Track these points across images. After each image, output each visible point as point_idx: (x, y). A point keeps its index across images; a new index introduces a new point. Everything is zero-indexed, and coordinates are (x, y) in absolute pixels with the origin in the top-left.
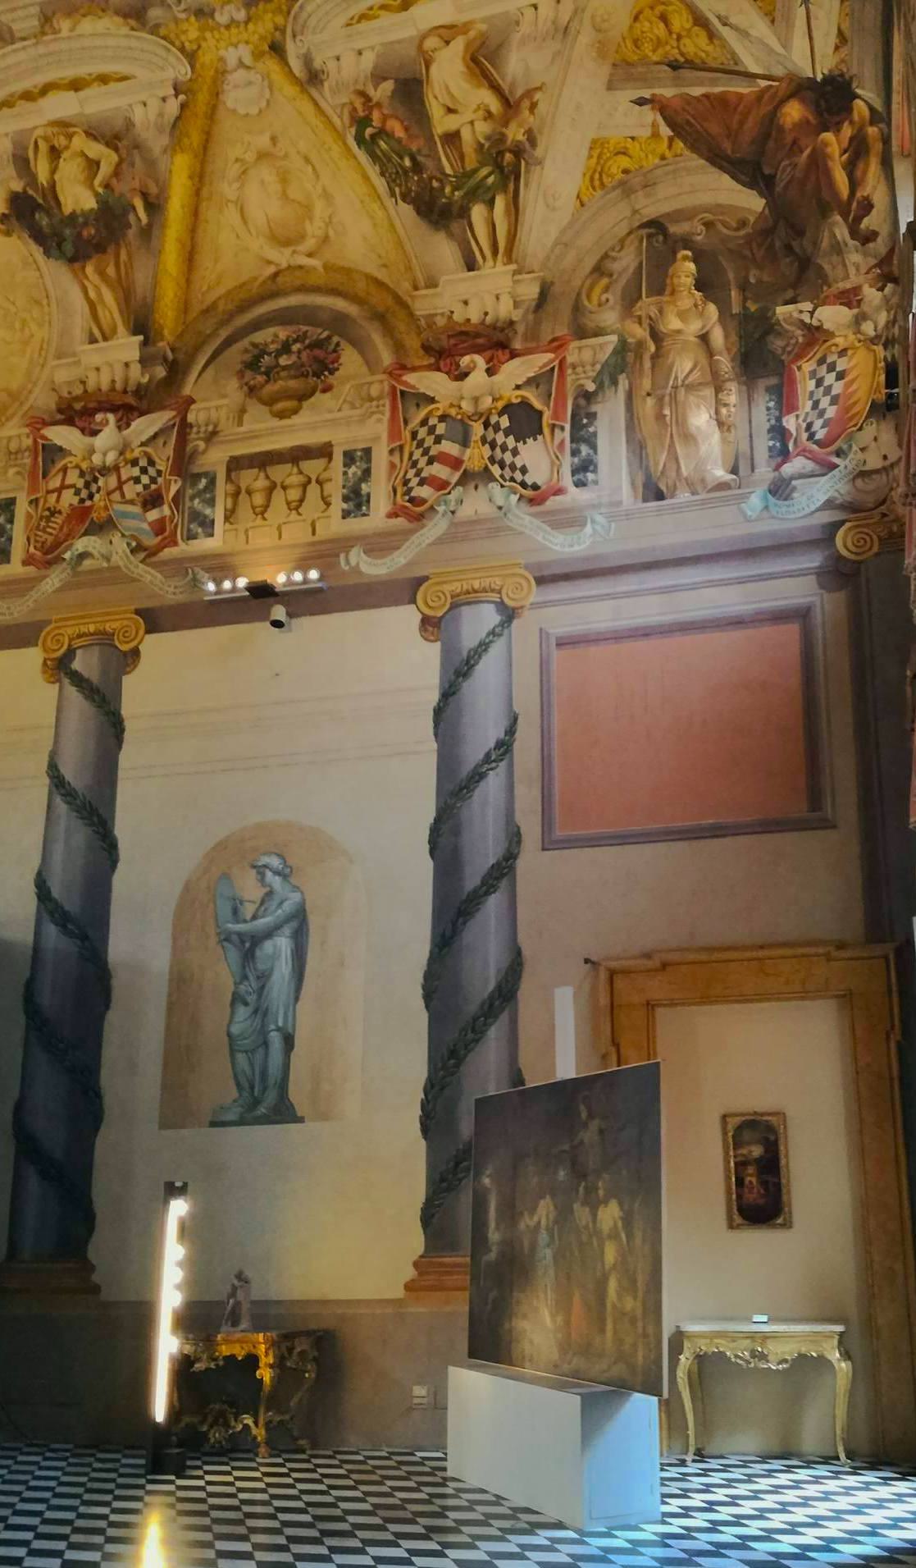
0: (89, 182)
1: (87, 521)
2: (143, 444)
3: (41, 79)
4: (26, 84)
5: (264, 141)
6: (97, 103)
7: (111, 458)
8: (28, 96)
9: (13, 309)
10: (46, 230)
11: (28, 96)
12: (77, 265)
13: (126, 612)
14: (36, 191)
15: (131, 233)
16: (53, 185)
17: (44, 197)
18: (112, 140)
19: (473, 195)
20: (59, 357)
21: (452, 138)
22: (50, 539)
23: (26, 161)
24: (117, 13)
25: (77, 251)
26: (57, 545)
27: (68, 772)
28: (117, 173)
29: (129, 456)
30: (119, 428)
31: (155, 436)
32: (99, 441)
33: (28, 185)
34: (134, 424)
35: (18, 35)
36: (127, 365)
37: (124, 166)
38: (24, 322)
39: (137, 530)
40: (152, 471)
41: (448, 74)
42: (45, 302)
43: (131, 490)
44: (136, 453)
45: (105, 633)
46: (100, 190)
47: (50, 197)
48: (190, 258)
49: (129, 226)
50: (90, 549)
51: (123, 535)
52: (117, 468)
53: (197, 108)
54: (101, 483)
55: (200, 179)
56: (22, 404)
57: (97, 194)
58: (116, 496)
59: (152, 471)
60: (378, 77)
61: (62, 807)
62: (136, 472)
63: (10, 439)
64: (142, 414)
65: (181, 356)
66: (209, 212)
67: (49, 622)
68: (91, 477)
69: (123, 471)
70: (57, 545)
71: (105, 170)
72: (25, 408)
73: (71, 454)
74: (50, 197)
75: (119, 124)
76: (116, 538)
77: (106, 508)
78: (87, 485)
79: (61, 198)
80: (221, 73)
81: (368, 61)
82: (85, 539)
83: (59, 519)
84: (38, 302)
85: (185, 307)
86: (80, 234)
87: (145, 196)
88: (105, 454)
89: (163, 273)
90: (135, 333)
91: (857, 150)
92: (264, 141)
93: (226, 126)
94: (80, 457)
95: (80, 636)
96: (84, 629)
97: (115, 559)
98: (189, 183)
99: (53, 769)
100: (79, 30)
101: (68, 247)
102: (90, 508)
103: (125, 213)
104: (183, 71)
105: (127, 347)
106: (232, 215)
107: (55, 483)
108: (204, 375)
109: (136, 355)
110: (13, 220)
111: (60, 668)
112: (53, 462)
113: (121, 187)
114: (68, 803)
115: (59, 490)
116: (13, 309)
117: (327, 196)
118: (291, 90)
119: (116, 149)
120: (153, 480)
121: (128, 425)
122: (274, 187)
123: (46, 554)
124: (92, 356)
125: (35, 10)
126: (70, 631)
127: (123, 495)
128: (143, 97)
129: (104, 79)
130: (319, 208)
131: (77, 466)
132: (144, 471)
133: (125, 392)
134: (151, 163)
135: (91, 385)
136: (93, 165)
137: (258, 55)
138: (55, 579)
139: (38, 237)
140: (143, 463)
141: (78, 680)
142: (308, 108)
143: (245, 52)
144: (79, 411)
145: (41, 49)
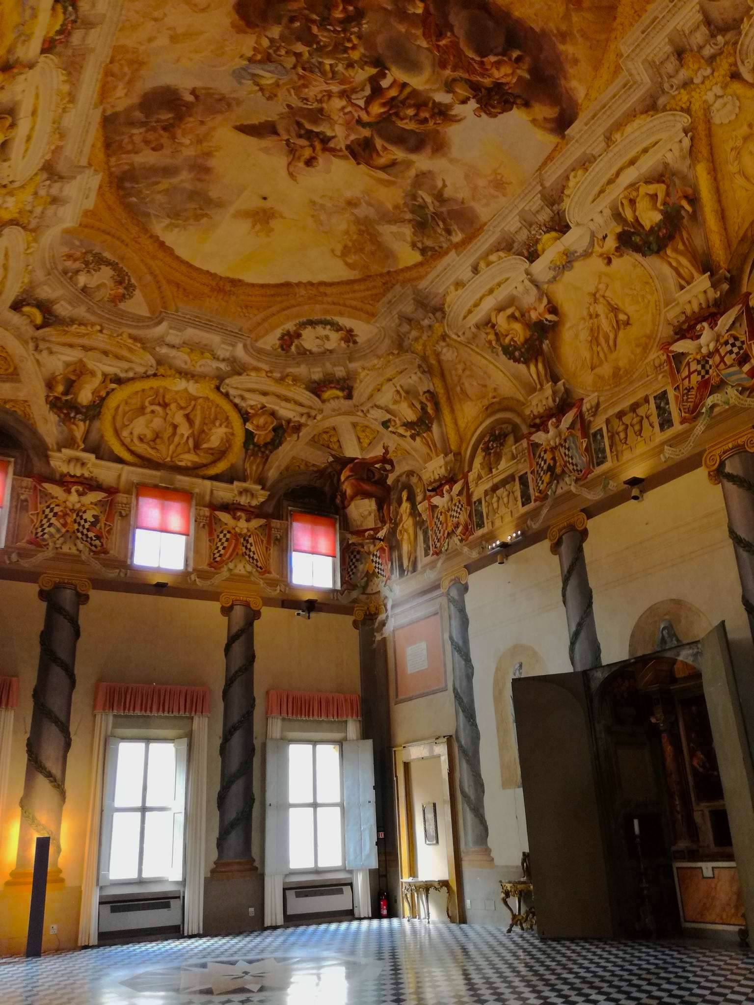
0: (654, 207)
1: (707, 387)
2: (728, 331)
3: (614, 170)
4: (608, 176)
6: (647, 164)
7: (712, 346)
8: (610, 182)
9: (635, 293)
10: (640, 243)
11: (610, 182)
12: (662, 253)
13: (747, 430)
14: (628, 225)
15: (685, 221)
16: (637, 220)
17: (634, 227)
18: (659, 178)
20: (667, 305)
22: (692, 404)
23: (619, 214)
24: (642, 113)
25: (659, 246)
26: (696, 406)
27: (742, 533)
28: (668, 194)
29: (722, 341)
30: (712, 328)
31: (734, 323)
32: (703, 340)
33: (624, 226)
34: (719, 322)
35: (597, 155)
36: (705, 292)
37: (671, 188)
38: (643, 297)
39: (738, 380)
40: (738, 344)
42: (651, 281)
43: (728, 360)
44: (726, 337)
45: (738, 446)
46: (662, 208)
47: (636, 226)
48: (722, 216)
49: (684, 217)
50: (716, 402)
51: (732, 387)
52: (717, 351)
54: (711, 362)
56: (655, 339)
57: (661, 211)
58: (722, 366)
59: (738, 344)
61: (744, 555)
62: (729, 347)
63: (654, 360)
64: (722, 315)
65: (734, 273)
67: (705, 450)
68: (704, 361)
69: (721, 350)
70: (696, 406)
71: (661, 196)
72: (658, 339)
73: (688, 354)
74: (636, 226)
75: (661, 168)
76: (729, 390)
77: (718, 375)
78: (703, 367)
79: (643, 223)
82: (711, 397)
83: (693, 392)
84: (647, 283)
85: (729, 245)
86: (658, 235)
87: (686, 197)
88: (708, 346)
89: (712, 235)
90: (704, 272)
94: (694, 353)
95: (724, 453)
96: (726, 448)
97: (732, 401)
98: (709, 176)
99: (732, 533)
100: (625, 134)
101: (654, 247)
102: (709, 378)
103: (678, 212)
105: (703, 282)
107: (685, 373)
108: (752, 275)
109: (709, 284)
110: (622, 248)
111: (719, 474)
112: (681, 363)
113: (671, 200)
114: (747, 551)
115: (689, 376)
116: (635, 293)
119: (663, 182)
120: (740, 348)
121: (716, 324)
123: (692, 413)
124: (683, 297)
125: (602, 138)
126: (718, 451)
127: (725, 364)
128: (669, 147)
129: (645, 151)
131: (695, 359)
132: (733, 345)
133: (709, 307)
134: (684, 178)
135: (689, 312)
136: (654, 197)
138: (700, 427)
139: (637, 249)
140: (731, 341)
141: (730, 477)
144: (686, 329)
145: (610, 155)
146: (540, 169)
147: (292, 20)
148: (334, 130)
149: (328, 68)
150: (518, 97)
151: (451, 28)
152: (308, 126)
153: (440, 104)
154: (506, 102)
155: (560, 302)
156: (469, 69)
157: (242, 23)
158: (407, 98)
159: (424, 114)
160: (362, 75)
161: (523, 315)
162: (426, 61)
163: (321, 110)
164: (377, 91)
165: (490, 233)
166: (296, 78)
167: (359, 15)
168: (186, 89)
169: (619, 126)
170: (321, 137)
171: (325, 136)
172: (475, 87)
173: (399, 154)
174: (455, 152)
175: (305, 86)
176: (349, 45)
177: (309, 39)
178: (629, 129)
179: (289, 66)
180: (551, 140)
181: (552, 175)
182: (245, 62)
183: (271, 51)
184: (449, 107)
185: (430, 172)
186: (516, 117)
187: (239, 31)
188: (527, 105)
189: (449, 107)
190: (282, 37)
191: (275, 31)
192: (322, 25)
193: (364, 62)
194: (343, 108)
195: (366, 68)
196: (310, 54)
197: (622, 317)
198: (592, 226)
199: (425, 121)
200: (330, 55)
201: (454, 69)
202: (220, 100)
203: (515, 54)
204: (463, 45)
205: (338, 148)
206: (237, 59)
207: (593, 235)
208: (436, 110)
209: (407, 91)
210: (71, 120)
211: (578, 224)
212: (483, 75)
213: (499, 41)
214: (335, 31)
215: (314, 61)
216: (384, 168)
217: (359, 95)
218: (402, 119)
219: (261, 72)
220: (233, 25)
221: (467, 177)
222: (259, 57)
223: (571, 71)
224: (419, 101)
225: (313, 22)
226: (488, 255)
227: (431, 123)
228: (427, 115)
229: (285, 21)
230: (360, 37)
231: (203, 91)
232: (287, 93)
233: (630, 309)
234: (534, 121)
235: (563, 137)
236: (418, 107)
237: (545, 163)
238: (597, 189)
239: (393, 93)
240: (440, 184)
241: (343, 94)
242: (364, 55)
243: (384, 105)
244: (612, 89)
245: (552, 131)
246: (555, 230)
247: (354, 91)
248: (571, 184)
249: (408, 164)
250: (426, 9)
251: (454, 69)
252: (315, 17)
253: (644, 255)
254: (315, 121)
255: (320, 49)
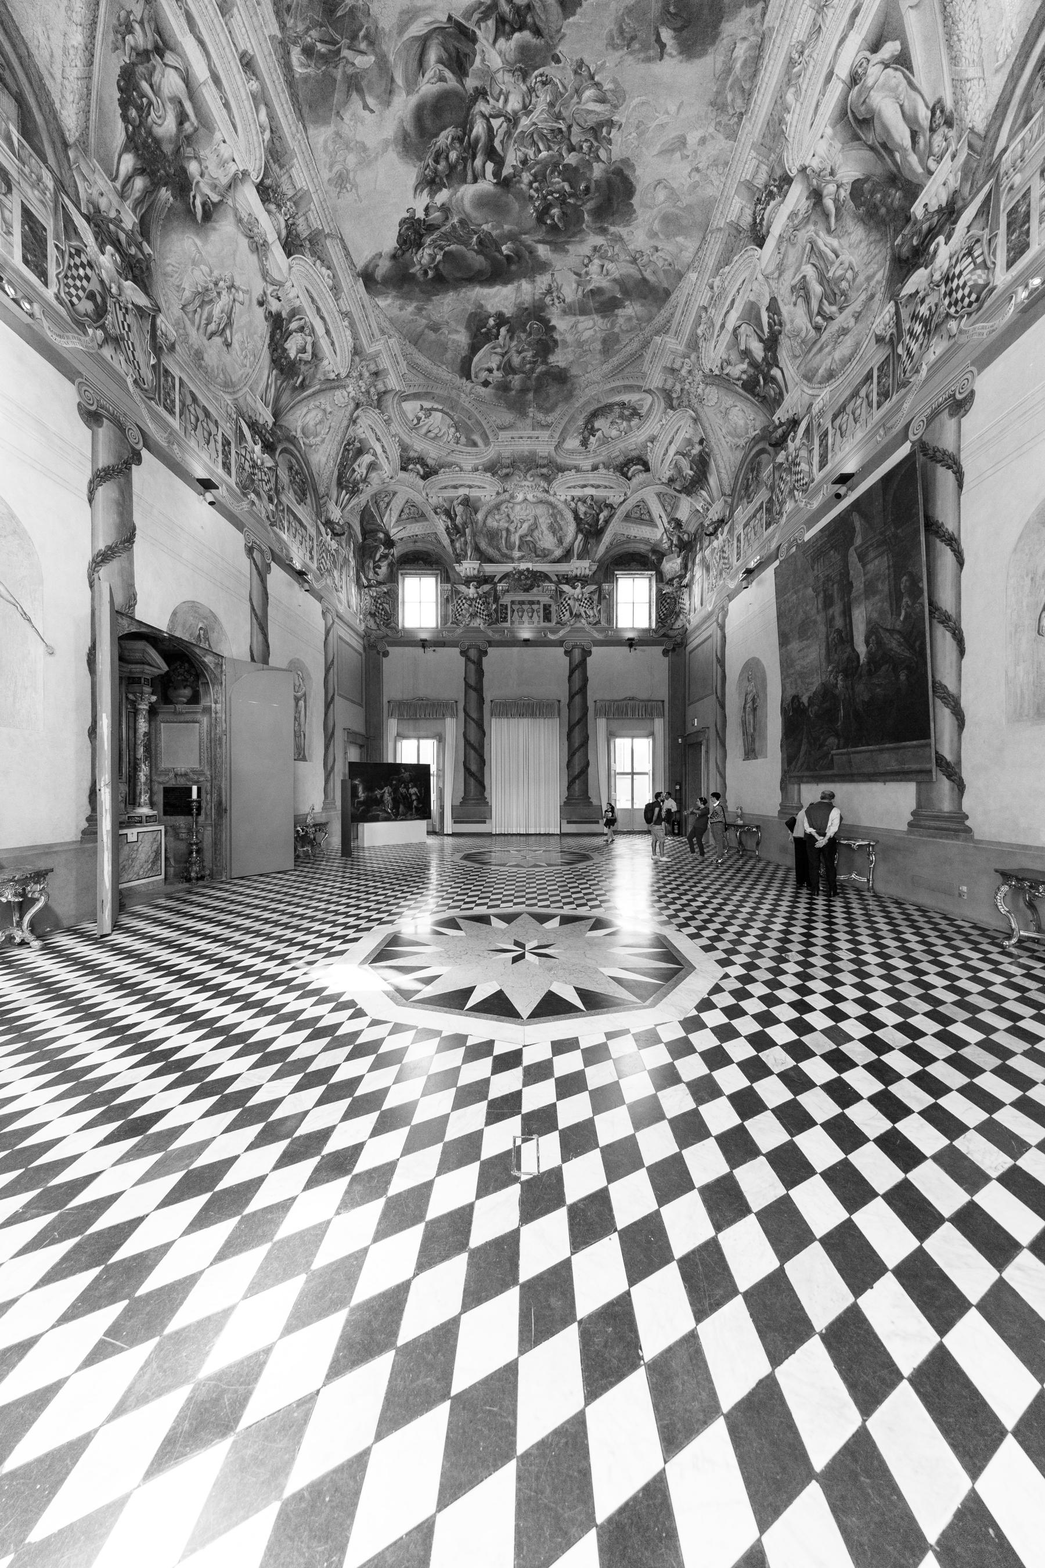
3: (326, 315)
4: (323, 310)
5: (329, 410)
6: (324, 343)
8: (318, 310)
11: (318, 310)
19: (347, 487)
21: (354, 471)
28: (306, 362)
41: (366, 459)
53: (334, 384)
55: (314, 394)
60: (360, 441)
66: (304, 403)
75: (320, 356)
80: (344, 387)
81: (363, 436)
87: (304, 380)
91: (384, 557)
92: (329, 410)
93: (329, 394)
104: (343, 375)
105: (271, 420)
106: (305, 410)
113: (303, 368)
117: (323, 441)
118: (348, 414)
122: (317, 419)
129: (333, 344)
130: (319, 439)
134: (314, 376)
137: (353, 398)
142: (345, 423)
143: (353, 394)
146: (342, 240)
147: (587, 189)
148: (500, 53)
149: (541, 147)
150: (404, 253)
151: (478, 253)
152: (526, 35)
153: (440, 190)
154: (405, 242)
155: (217, 226)
156: (445, 236)
157: (626, 172)
158: (465, 167)
159: (442, 166)
160: (512, 159)
161: (188, 138)
162: (476, 215)
163: (525, 75)
164: (491, 153)
165: (293, 128)
166: (565, 114)
167: (541, 218)
168: (671, 55)
169: (352, 325)
170: (507, 28)
171: (504, 33)
172: (431, 228)
173: (428, 87)
174: (392, 155)
175: (551, 105)
176: (535, 185)
177: (571, 174)
178: (348, 333)
179: (575, 129)
180: (360, 264)
181: (333, 248)
182: (615, 118)
183: (596, 144)
184: (432, 194)
185: (388, 104)
186: (389, 242)
187: (626, 161)
188: (394, 257)
189: (432, 194)
190: (589, 165)
191: (597, 171)
192: (563, 193)
193: (516, 174)
194: (506, 101)
195: (511, 171)
196: (561, 155)
197: (228, 332)
198: (288, 284)
199: (437, 162)
200: (545, 164)
201: (453, 226)
202: (633, 38)
203: (431, 273)
204: (462, 248)
205: (483, 25)
206: (624, 121)
207: (281, 285)
208: (437, 180)
209: (470, 177)
210: (800, 30)
211: (290, 268)
212: (434, 241)
213: (444, 270)
214: (551, 193)
215: (556, 148)
216: (424, 42)
217: (501, 131)
218: (453, 139)
219: (598, 107)
220: (632, 167)
221: (364, 148)
222: (604, 130)
223: (398, 302)
224: (456, 175)
225: (571, 195)
226: (266, 105)
227: (431, 162)
228: (440, 167)
229: (593, 186)
230: (531, 197)
231: (652, 53)
232: (566, 82)
233: (236, 345)
234: (380, 255)
235: (359, 275)
236: (452, 168)
237: (345, 248)
238: (315, 296)
239: (478, 162)
240: (371, 101)
241: (513, 121)
242: (520, 182)
243: (477, 140)
244: (374, 325)
245: (367, 267)
246: (287, 237)
247: (508, 134)
248: (324, 270)
249: (411, 86)
250: (501, 252)
251: (453, 226)
252: (571, 201)
253: (270, 345)
254: (524, 50)
255: (556, 165)
